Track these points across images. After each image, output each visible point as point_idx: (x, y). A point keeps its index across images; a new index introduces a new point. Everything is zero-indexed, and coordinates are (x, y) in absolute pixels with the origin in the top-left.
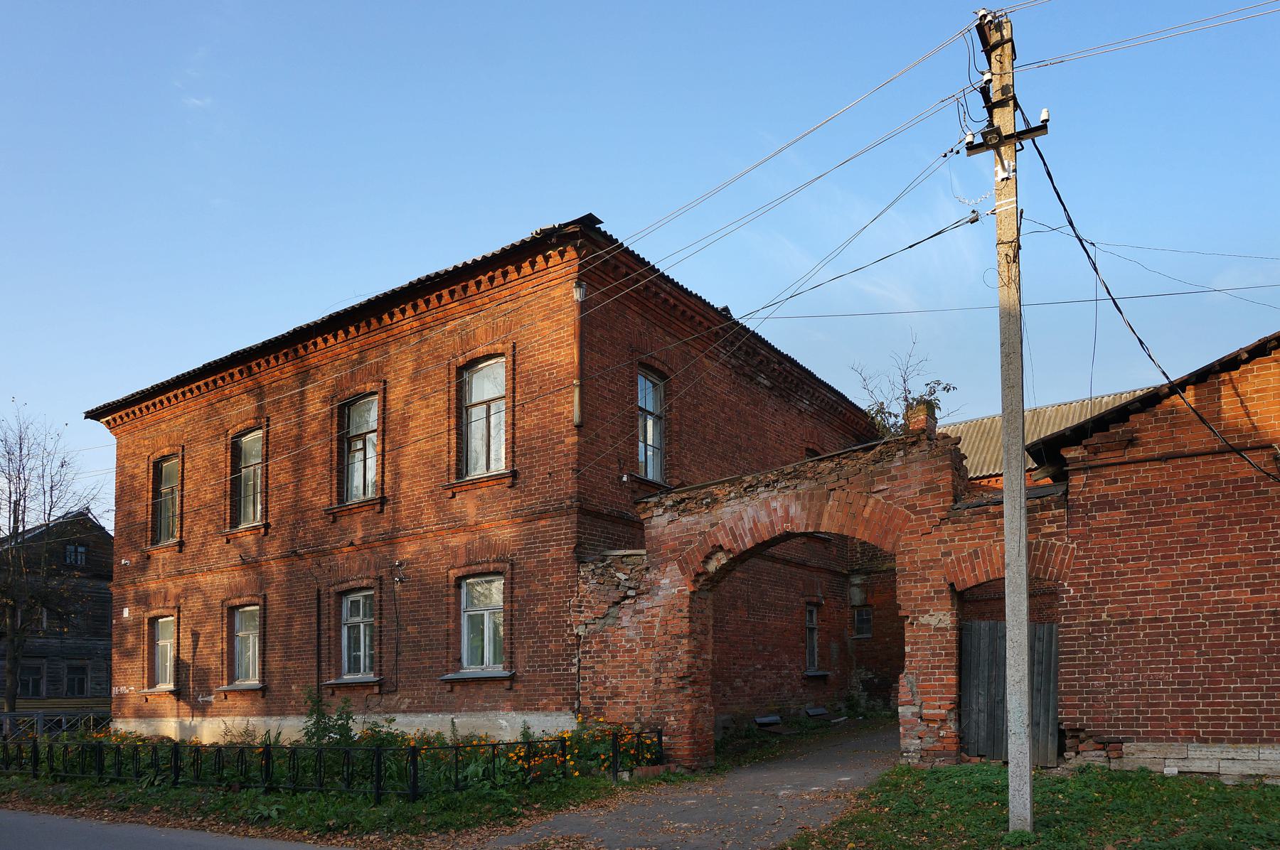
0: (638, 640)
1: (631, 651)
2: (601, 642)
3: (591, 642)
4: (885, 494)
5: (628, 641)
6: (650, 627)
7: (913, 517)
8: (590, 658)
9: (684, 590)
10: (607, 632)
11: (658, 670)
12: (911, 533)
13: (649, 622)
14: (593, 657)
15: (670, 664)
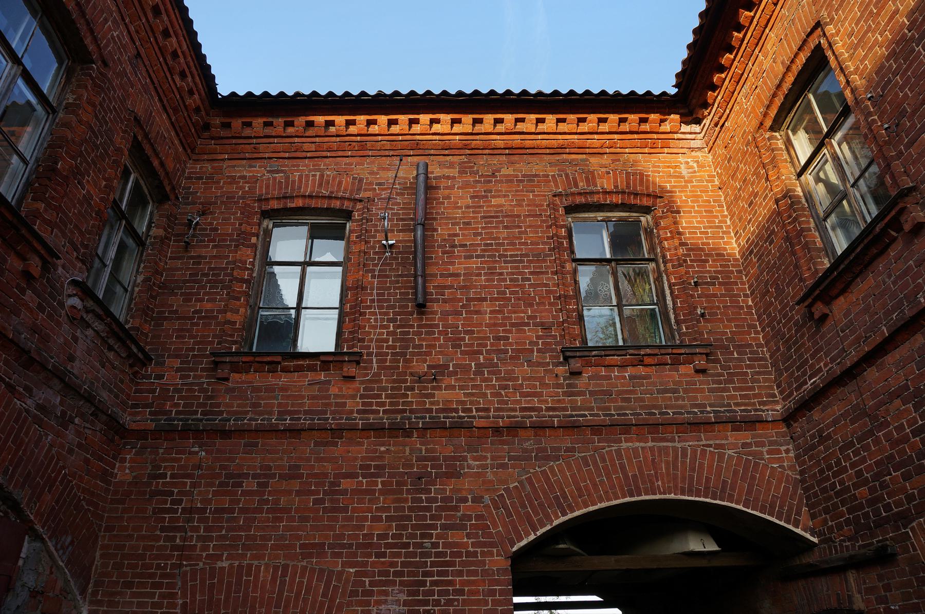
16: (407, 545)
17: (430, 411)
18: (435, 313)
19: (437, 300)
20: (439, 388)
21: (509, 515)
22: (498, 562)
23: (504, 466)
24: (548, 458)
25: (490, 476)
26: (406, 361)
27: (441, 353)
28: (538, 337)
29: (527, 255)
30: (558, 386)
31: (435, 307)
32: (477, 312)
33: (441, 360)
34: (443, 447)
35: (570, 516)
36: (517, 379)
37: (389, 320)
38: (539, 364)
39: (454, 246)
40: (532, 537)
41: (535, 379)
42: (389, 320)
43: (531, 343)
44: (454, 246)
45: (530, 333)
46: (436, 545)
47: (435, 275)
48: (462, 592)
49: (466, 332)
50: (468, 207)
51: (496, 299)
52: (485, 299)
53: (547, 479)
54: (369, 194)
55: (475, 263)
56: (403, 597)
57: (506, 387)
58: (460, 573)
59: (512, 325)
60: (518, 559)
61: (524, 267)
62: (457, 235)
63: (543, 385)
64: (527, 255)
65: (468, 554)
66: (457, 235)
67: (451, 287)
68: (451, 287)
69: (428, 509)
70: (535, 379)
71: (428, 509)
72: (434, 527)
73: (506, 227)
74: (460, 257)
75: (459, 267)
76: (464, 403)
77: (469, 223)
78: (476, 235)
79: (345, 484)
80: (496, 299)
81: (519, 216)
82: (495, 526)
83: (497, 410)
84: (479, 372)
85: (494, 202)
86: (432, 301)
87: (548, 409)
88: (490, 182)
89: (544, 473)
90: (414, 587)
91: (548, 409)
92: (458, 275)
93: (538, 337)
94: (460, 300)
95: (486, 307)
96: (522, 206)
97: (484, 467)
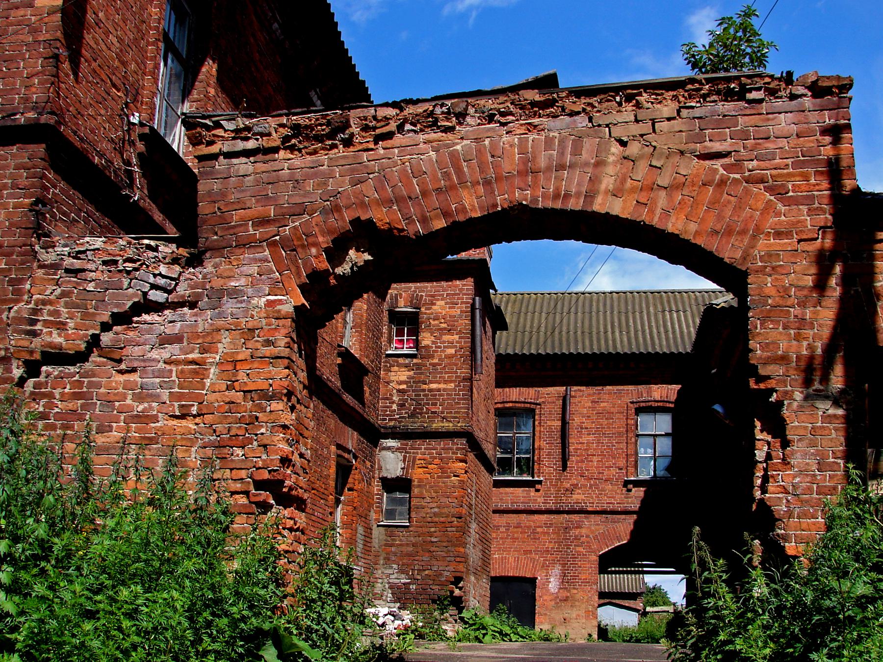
0: (165, 397)
1: (144, 418)
2: (76, 396)
3: (51, 396)
4: (726, 161)
5: (139, 398)
6: (196, 373)
7: (779, 206)
8: (47, 427)
9: (280, 302)
10: (94, 376)
11: (207, 462)
12: (778, 234)
13: (193, 362)
14: (53, 427)
15: (239, 452)
16: (561, 551)
17: (570, 503)
18: (573, 461)
19: (574, 455)
20: (574, 494)
21: (599, 542)
22: (594, 558)
23: (597, 525)
24: (615, 522)
25: (593, 528)
26: (561, 482)
27: (575, 479)
28: (616, 473)
29: (615, 434)
30: (623, 494)
31: (574, 459)
32: (592, 461)
33: (575, 482)
34: (575, 517)
35: (621, 543)
36: (605, 491)
37: (554, 464)
38: (615, 485)
39: (582, 428)
40: (607, 550)
41: (613, 491)
42: (554, 464)
43: (613, 475)
44: (582, 428)
45: (613, 471)
46: (572, 552)
47: (573, 443)
48: (580, 567)
49: (587, 470)
50: (589, 408)
51: (600, 455)
52: (595, 455)
53: (614, 529)
54: (543, 400)
55: (591, 438)
56: (560, 568)
57: (601, 494)
58: (580, 561)
59: (606, 467)
60: (602, 558)
61: (613, 440)
62: (584, 423)
63: (616, 493)
64: (615, 434)
65: (583, 555)
66: (584, 423)
67: (581, 449)
68: (581, 449)
69: (569, 539)
70: (613, 491)
71: (569, 539)
72: (571, 545)
73: (606, 419)
74: (584, 434)
75: (584, 439)
76: (584, 500)
77: (589, 417)
78: (592, 423)
79: (539, 530)
80: (600, 455)
81: (613, 413)
82: (593, 545)
83: (597, 503)
84: (591, 487)
85: (602, 405)
86: (572, 456)
87: (617, 503)
88: (600, 393)
89: (613, 527)
90: (564, 565)
91: (617, 503)
92: (584, 443)
93: (616, 473)
94: (584, 455)
95: (595, 459)
96: (614, 407)
97: (591, 525)
